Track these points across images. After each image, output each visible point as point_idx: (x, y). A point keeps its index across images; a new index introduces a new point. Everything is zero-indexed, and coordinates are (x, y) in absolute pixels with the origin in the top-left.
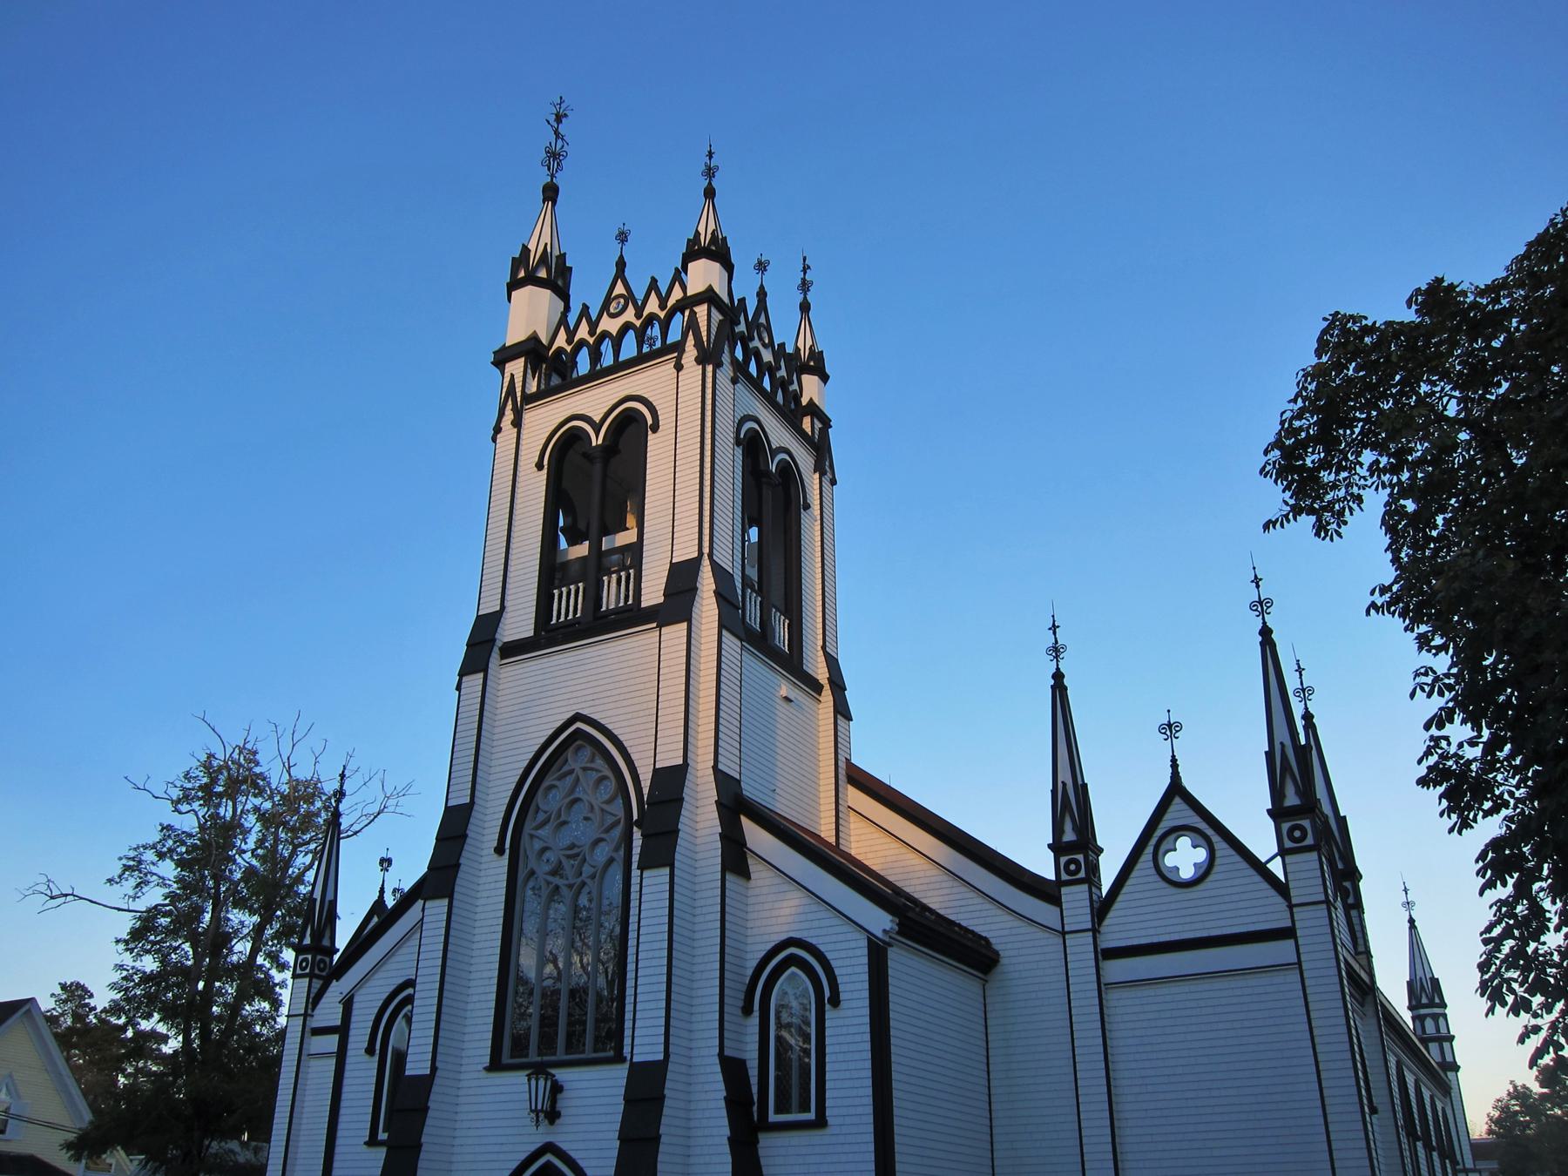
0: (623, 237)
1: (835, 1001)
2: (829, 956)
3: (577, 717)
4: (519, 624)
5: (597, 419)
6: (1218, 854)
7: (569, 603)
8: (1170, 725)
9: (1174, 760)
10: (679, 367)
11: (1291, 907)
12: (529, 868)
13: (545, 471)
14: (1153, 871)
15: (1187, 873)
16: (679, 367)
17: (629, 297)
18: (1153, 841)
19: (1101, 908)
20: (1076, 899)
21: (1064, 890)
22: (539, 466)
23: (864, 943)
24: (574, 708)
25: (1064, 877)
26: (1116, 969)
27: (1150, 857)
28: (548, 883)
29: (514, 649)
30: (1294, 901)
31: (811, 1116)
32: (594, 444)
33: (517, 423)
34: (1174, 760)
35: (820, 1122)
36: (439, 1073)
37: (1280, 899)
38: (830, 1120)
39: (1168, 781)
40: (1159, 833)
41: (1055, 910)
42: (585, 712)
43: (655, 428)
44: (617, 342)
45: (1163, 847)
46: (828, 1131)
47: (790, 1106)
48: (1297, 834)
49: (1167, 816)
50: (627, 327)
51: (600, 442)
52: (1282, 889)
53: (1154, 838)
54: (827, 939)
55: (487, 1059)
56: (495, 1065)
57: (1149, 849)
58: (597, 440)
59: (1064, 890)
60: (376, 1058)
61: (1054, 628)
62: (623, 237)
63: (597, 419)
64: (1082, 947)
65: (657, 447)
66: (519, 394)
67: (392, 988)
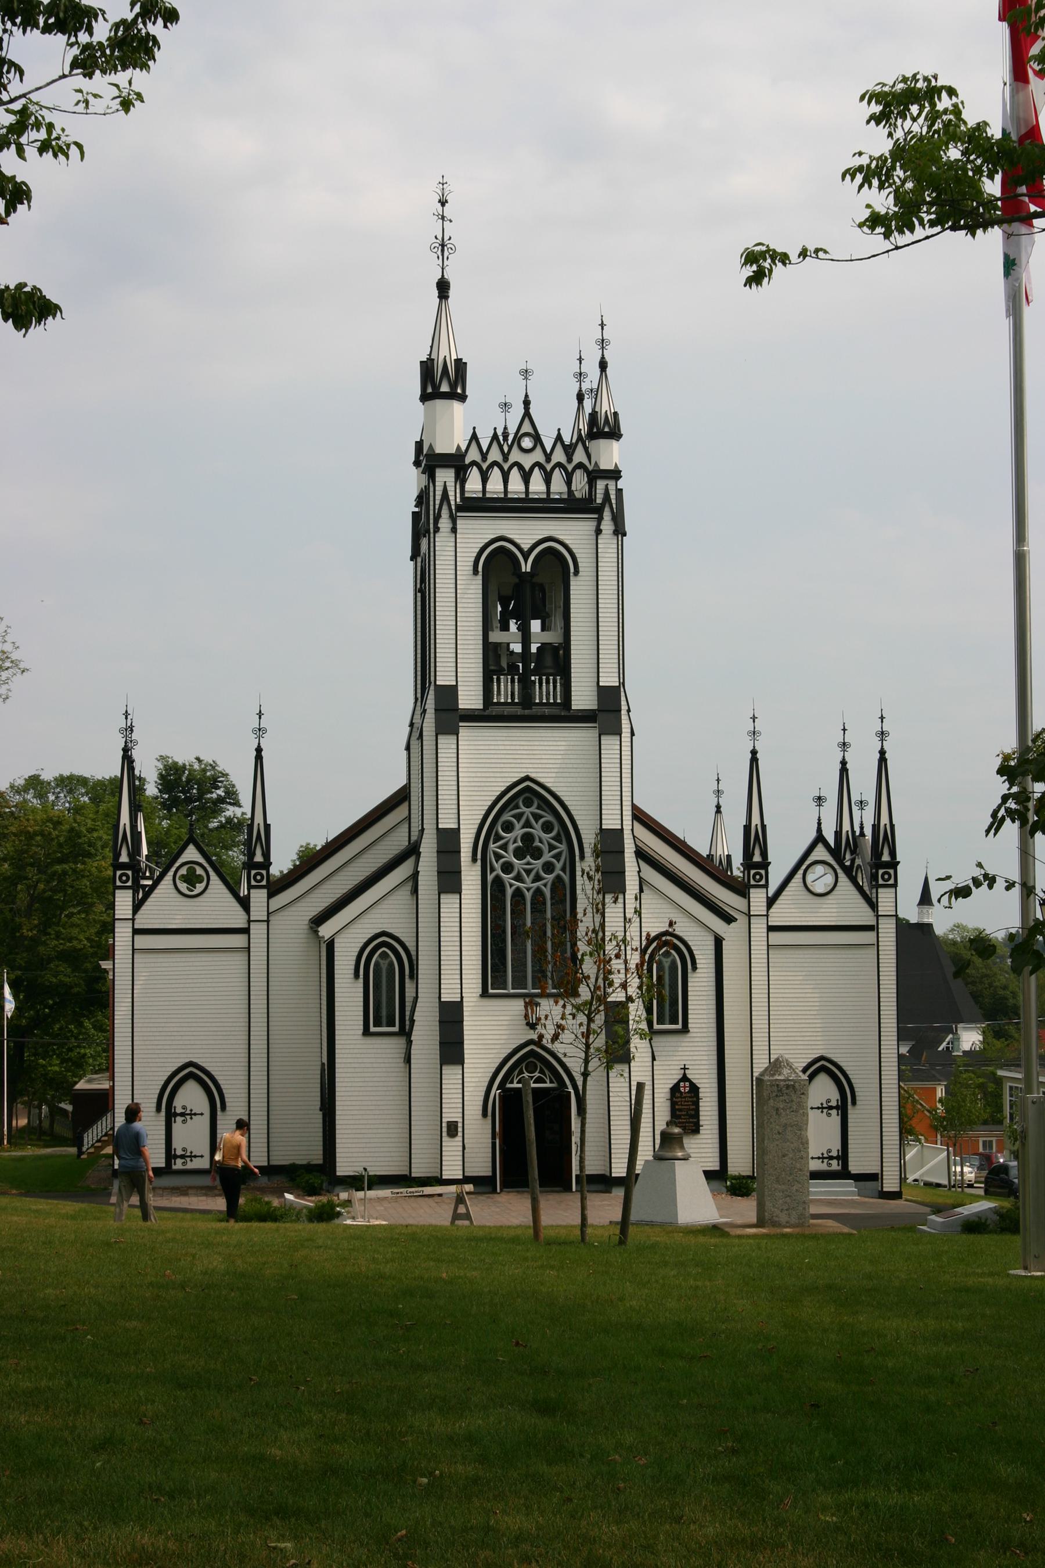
0: (526, 373)
1: (695, 968)
2: (690, 943)
3: (527, 778)
4: (470, 698)
5: (526, 547)
6: (839, 880)
7: (506, 690)
8: (819, 798)
9: (819, 819)
10: (598, 531)
11: (878, 916)
12: (494, 874)
13: (480, 577)
14: (802, 885)
15: (819, 888)
16: (598, 531)
17: (537, 438)
18: (804, 867)
19: (771, 902)
20: (758, 898)
21: (752, 890)
22: (475, 572)
23: (713, 938)
24: (525, 770)
25: (752, 882)
26: (776, 938)
27: (801, 876)
28: (511, 885)
29: (471, 717)
30: (880, 913)
31: (679, 1026)
32: (523, 570)
33: (454, 530)
34: (819, 819)
35: (685, 1029)
36: (464, 1000)
37: (869, 910)
38: (691, 1030)
39: (813, 834)
40: (807, 863)
41: (745, 901)
42: (532, 775)
43: (577, 572)
44: (526, 477)
45: (810, 870)
46: (690, 1035)
47: (664, 1020)
48: (886, 877)
49: (814, 854)
50: (537, 464)
51: (529, 570)
52: (873, 905)
53: (802, 864)
54: (689, 934)
55: (480, 991)
56: (485, 994)
57: (801, 872)
58: (526, 567)
59: (752, 890)
60: (361, 980)
61: (754, 718)
62: (526, 373)
63: (526, 547)
64: (759, 928)
65: (579, 589)
66: (453, 503)
67: (369, 936)
